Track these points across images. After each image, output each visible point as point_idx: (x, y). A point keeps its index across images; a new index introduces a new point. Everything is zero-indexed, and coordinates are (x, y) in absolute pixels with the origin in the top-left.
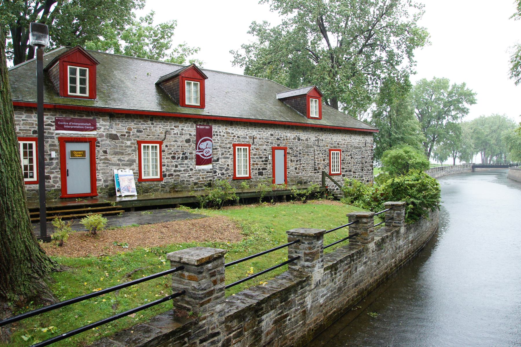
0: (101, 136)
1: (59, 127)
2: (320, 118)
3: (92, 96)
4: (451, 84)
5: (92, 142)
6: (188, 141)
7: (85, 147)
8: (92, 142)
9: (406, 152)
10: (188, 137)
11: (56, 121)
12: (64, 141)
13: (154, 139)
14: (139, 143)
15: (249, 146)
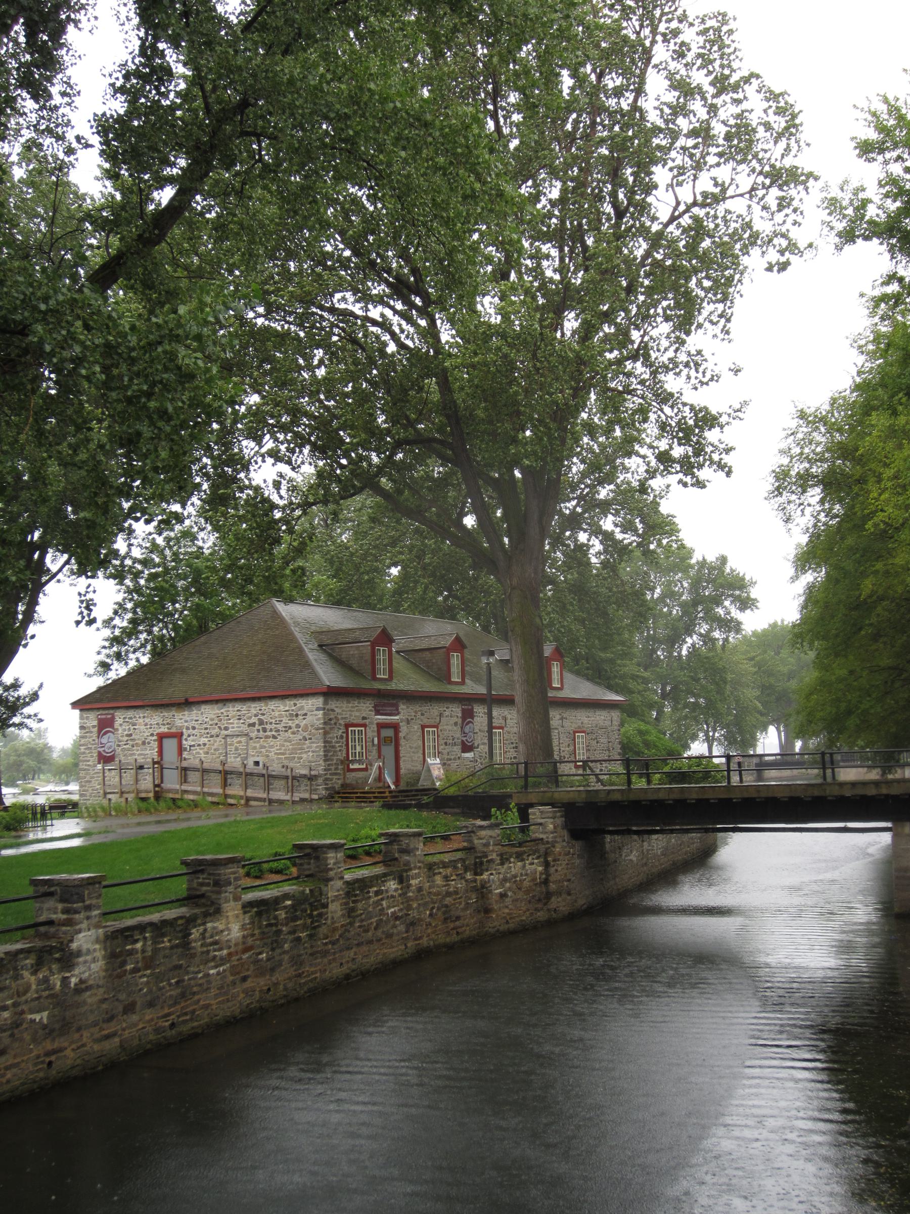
0: (402, 721)
1: (378, 713)
2: (561, 689)
3: (391, 678)
4: (696, 558)
5: (395, 727)
6: (456, 724)
7: (389, 733)
8: (395, 727)
9: (641, 733)
10: (455, 719)
11: (375, 707)
12: (381, 726)
13: (431, 722)
14: (423, 727)
15: (501, 728)
